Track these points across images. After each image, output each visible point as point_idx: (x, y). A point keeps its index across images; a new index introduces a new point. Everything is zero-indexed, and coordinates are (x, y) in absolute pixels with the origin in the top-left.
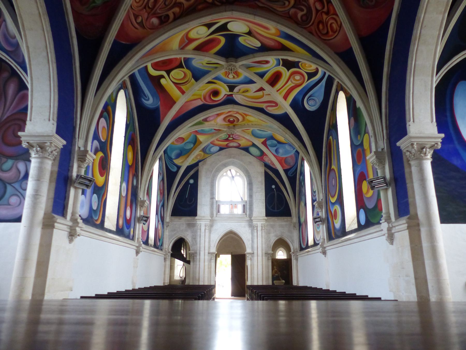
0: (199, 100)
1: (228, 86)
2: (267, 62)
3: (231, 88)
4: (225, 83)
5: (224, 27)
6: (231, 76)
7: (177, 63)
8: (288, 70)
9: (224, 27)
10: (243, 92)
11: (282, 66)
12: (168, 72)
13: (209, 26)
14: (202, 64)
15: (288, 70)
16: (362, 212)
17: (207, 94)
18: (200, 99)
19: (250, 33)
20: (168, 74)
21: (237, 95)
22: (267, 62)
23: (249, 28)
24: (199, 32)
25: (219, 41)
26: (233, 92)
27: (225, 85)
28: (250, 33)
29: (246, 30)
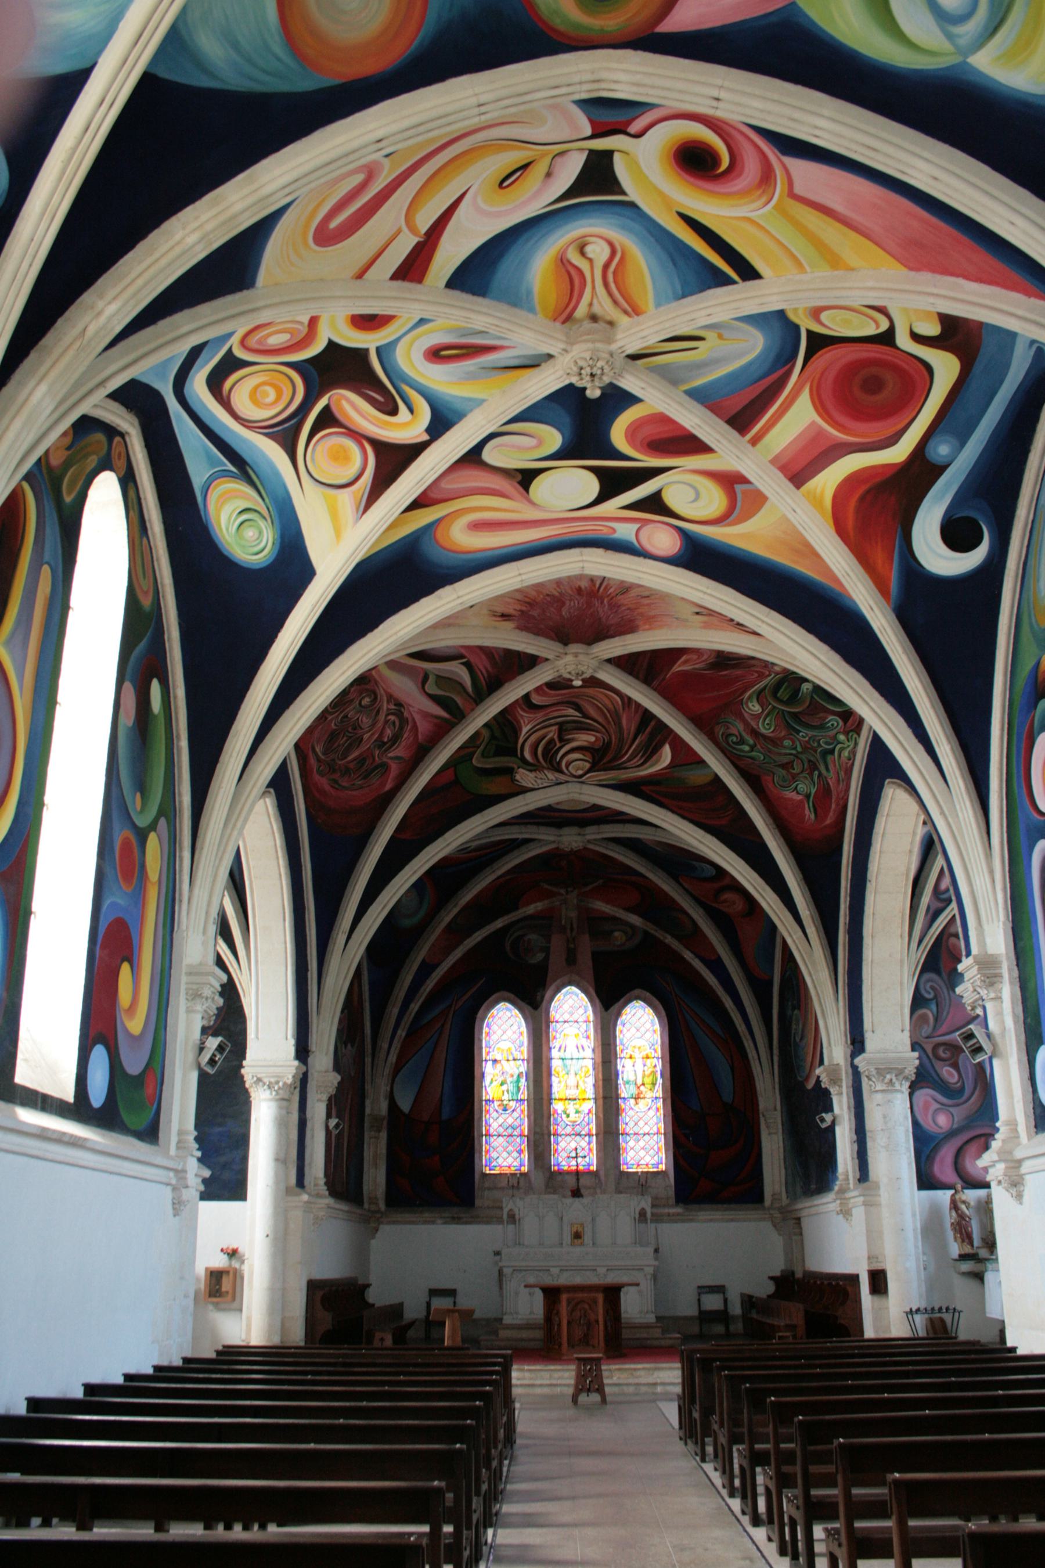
0: (798, 190)
1: (612, 185)
2: (436, 354)
3: (598, 177)
4: (632, 205)
5: (613, 483)
6: (599, 252)
7: (825, 357)
8: (332, 345)
9: (613, 483)
10: (525, 167)
11: (367, 350)
12: (887, 338)
13: (655, 504)
14: (720, 337)
15: (332, 345)
16: (99, 1055)
17: (744, 193)
18: (792, 195)
19: (526, 478)
20: (887, 338)
21: (565, 134)
22: (436, 354)
23: (532, 503)
24: (693, 496)
25: (632, 433)
26: (592, 153)
27: (633, 193)
28: (526, 478)
29: (540, 487)
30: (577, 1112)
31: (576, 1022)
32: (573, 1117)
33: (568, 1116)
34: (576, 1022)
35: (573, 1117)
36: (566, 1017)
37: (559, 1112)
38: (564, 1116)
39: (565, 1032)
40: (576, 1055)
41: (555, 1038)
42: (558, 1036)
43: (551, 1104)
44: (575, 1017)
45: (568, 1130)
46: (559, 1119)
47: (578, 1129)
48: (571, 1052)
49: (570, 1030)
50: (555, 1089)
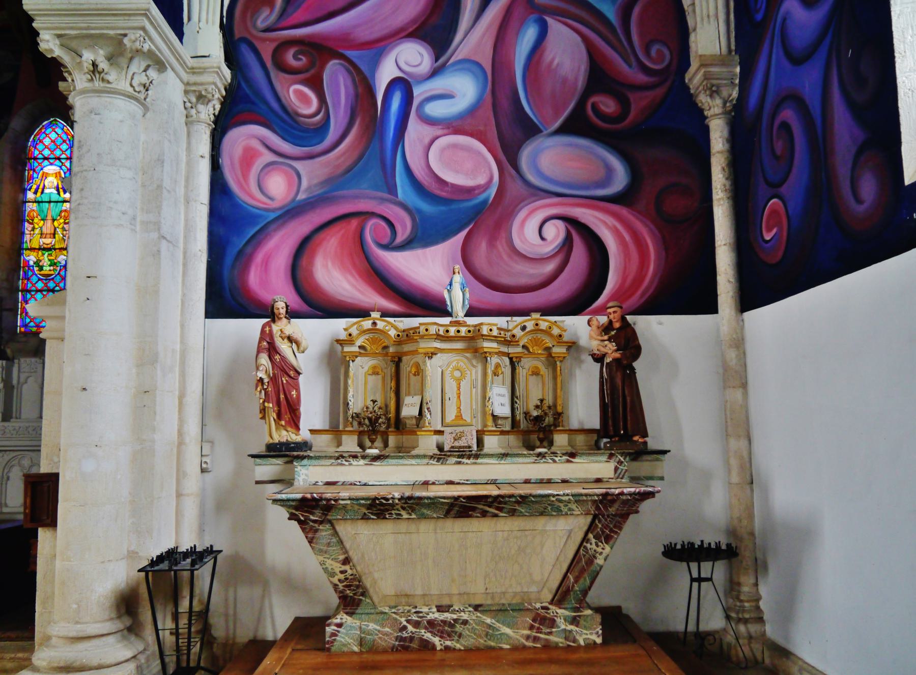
30: (53, 264)
31: (59, 159)
32: (47, 269)
33: (41, 268)
34: (59, 159)
35: (47, 269)
36: (46, 153)
37: (31, 263)
38: (36, 269)
39: (46, 170)
40: (55, 197)
41: (32, 178)
42: (35, 175)
43: (20, 254)
44: (58, 153)
45: (40, 285)
46: (30, 273)
47: (51, 285)
48: (50, 191)
49: (50, 169)
50: (27, 238)
